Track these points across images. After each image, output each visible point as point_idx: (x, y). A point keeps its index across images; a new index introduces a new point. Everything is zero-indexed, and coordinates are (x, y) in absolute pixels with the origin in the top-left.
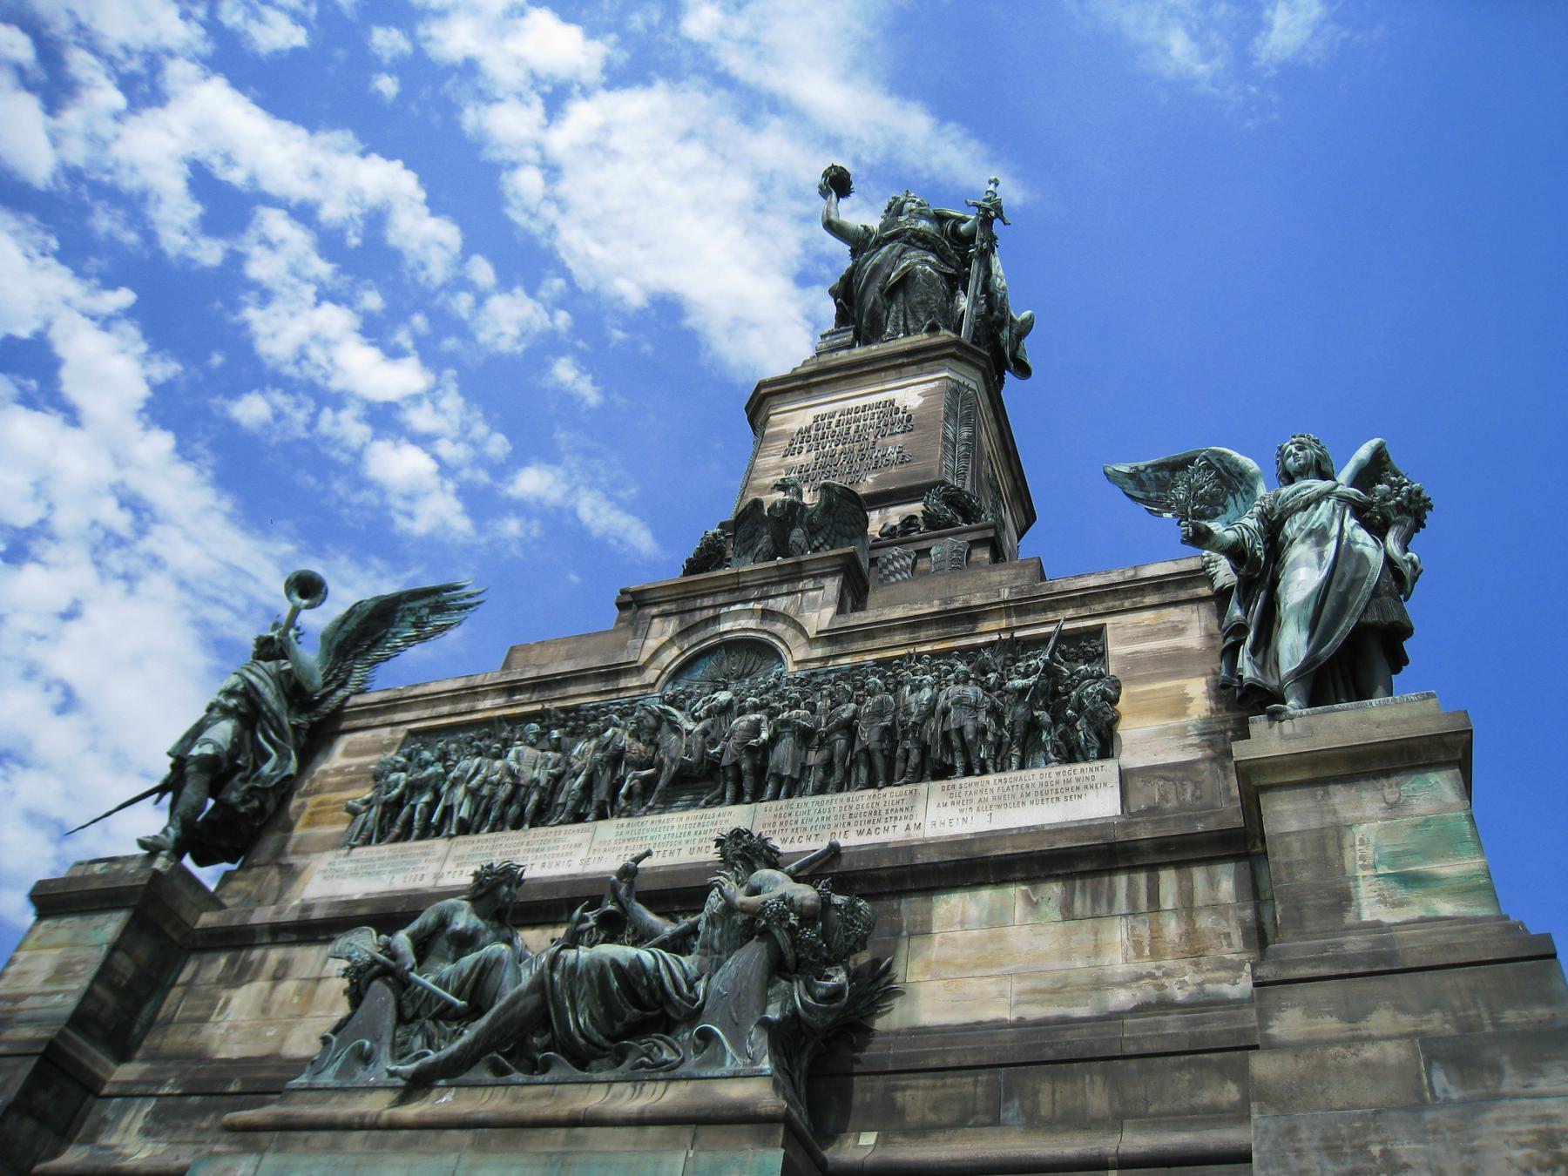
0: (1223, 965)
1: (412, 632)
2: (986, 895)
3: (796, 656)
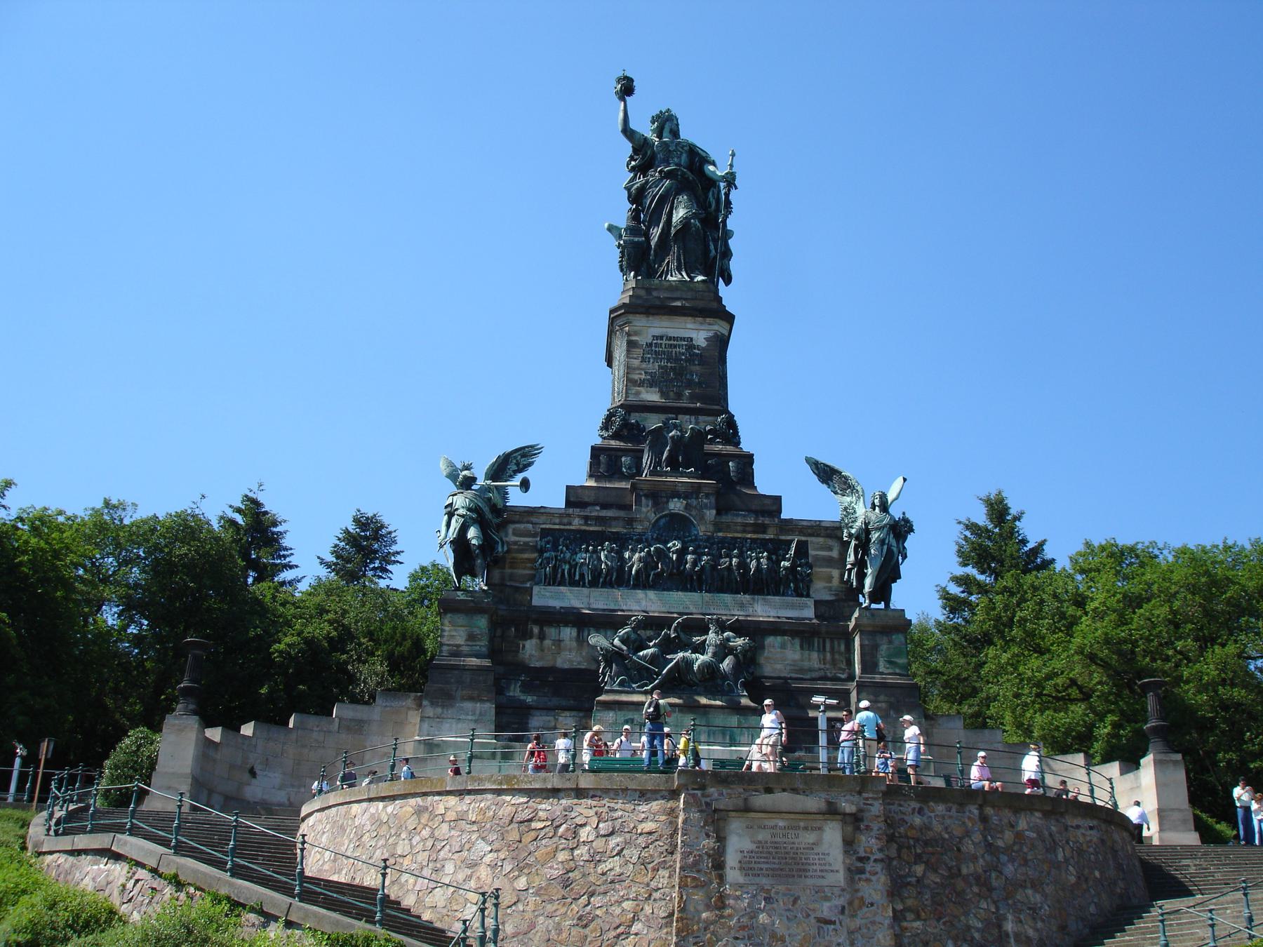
0: (840, 669)
1: (515, 468)
2: (779, 639)
3: (702, 530)
